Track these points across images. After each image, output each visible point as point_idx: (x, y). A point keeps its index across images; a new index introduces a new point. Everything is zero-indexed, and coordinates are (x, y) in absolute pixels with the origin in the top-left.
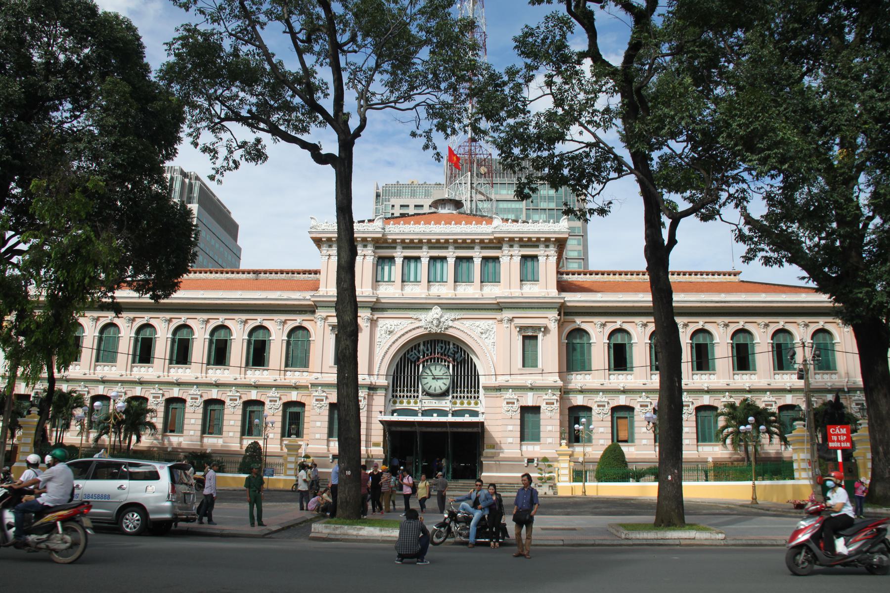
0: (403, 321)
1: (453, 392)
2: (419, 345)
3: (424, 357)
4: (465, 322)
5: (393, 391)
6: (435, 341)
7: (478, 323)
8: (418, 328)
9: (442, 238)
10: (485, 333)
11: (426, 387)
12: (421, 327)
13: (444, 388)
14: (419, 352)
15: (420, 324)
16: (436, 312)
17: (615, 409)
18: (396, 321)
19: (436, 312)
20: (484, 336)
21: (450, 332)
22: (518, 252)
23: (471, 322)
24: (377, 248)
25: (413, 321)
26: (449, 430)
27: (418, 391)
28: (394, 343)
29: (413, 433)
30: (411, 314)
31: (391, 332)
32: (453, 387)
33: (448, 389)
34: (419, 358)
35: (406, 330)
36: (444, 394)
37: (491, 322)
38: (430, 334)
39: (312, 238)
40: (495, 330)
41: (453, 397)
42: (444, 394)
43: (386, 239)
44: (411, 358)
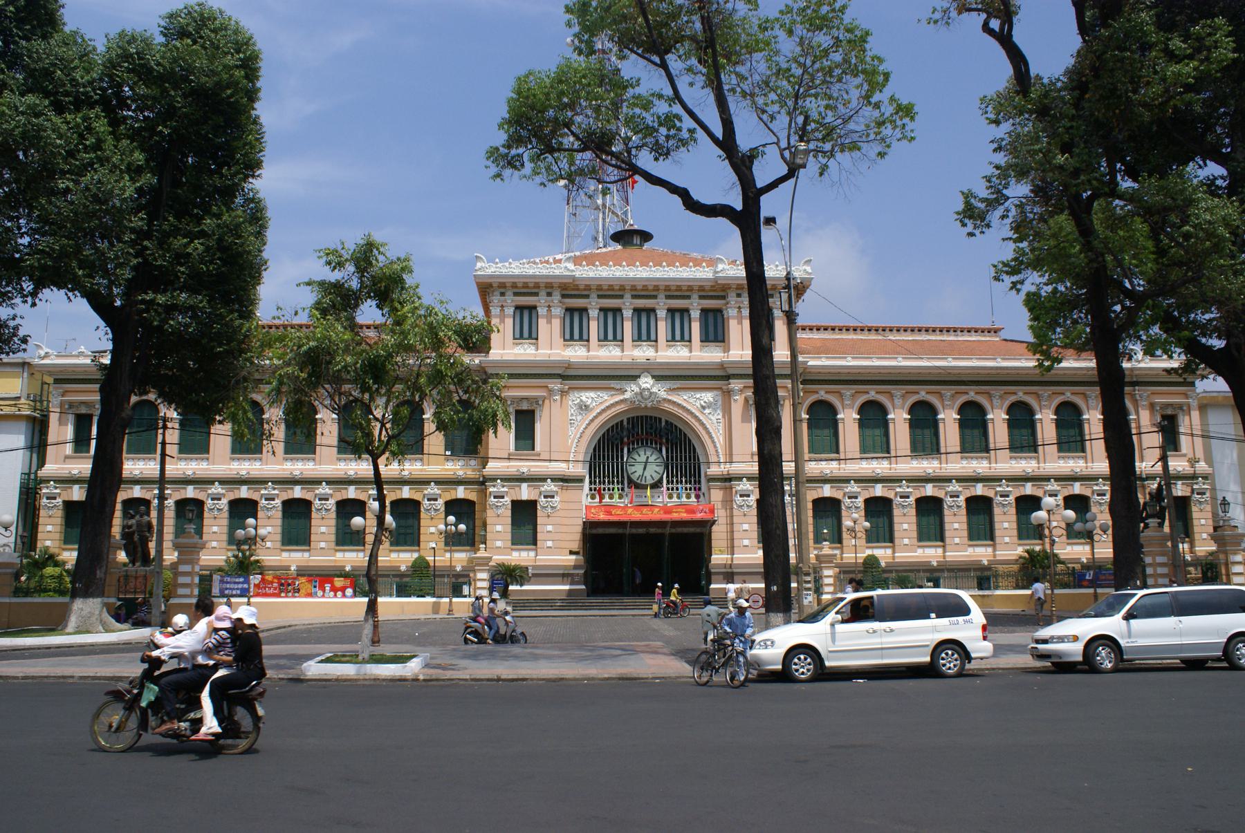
8: (622, 401)
9: (651, 285)
11: (634, 477)
13: (657, 477)
15: (627, 395)
16: (646, 382)
17: (870, 502)
18: (592, 394)
19: (646, 382)
20: (707, 411)
21: (667, 407)
24: (564, 296)
26: (628, 531)
28: (592, 421)
29: (619, 537)
30: (613, 384)
35: (607, 404)
36: (656, 485)
37: (716, 392)
42: (656, 485)
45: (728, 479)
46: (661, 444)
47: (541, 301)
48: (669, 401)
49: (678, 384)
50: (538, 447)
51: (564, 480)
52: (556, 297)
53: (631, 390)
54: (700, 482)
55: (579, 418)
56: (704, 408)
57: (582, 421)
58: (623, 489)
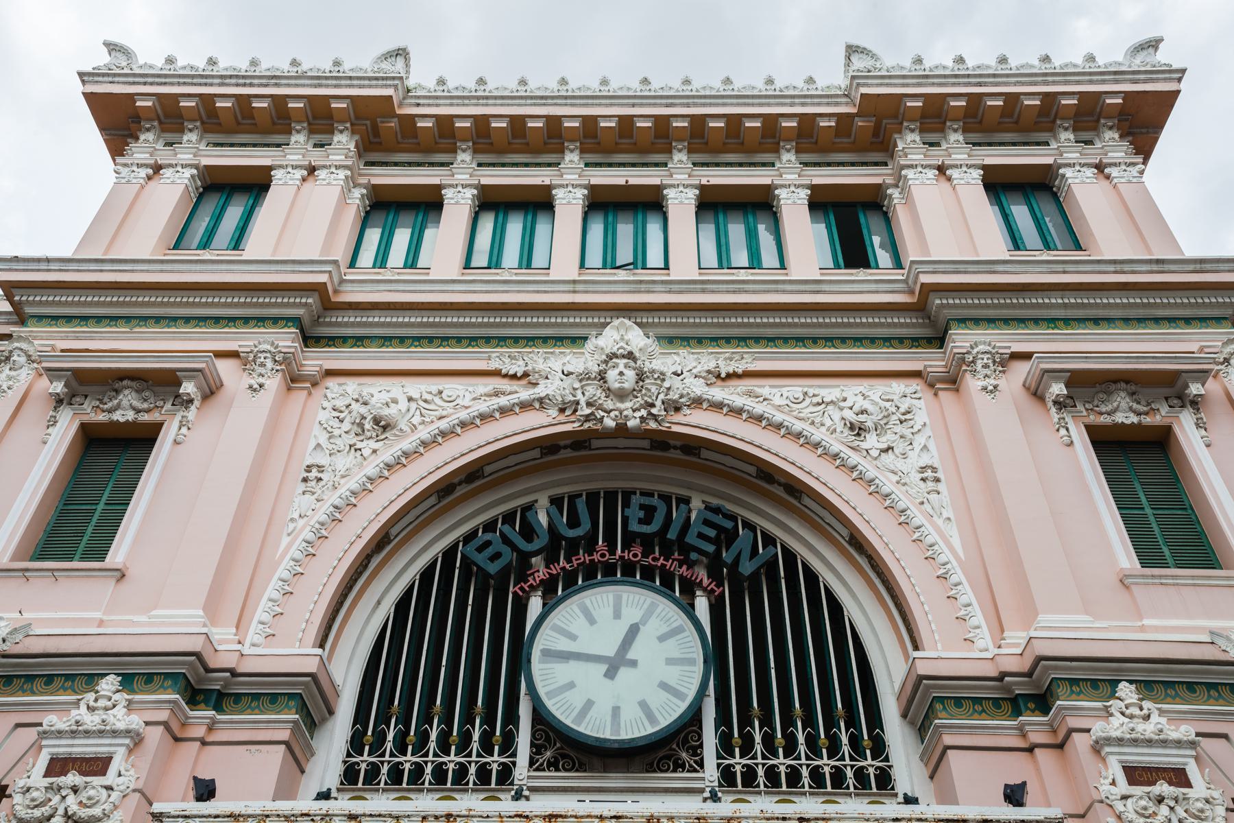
0: (453, 387)
1: (726, 747)
2: (529, 508)
3: (551, 560)
4: (765, 388)
5: (356, 744)
6: (611, 496)
7: (830, 391)
8: (525, 406)
10: (879, 429)
11: (563, 711)
12: (542, 403)
13: (669, 712)
14: (528, 531)
15: (550, 388)
18: (416, 387)
20: (872, 441)
22: (966, 158)
23: (795, 388)
25: (504, 384)
27: (508, 744)
31: (383, 426)
32: (723, 718)
33: (693, 719)
34: (523, 568)
37: (897, 387)
38: (579, 443)
39: (89, 97)
40: (920, 417)
41: (727, 776)
42: (665, 752)
43: (409, 121)
44: (480, 559)
45: (1033, 694)
46: (689, 589)
47: (287, 159)
48: (717, 406)
49: (750, 359)
50: (118, 554)
51: (203, 688)
52: (344, 143)
53: (558, 370)
54: (879, 748)
55: (344, 462)
56: (858, 430)
57: (349, 468)
58: (506, 774)
